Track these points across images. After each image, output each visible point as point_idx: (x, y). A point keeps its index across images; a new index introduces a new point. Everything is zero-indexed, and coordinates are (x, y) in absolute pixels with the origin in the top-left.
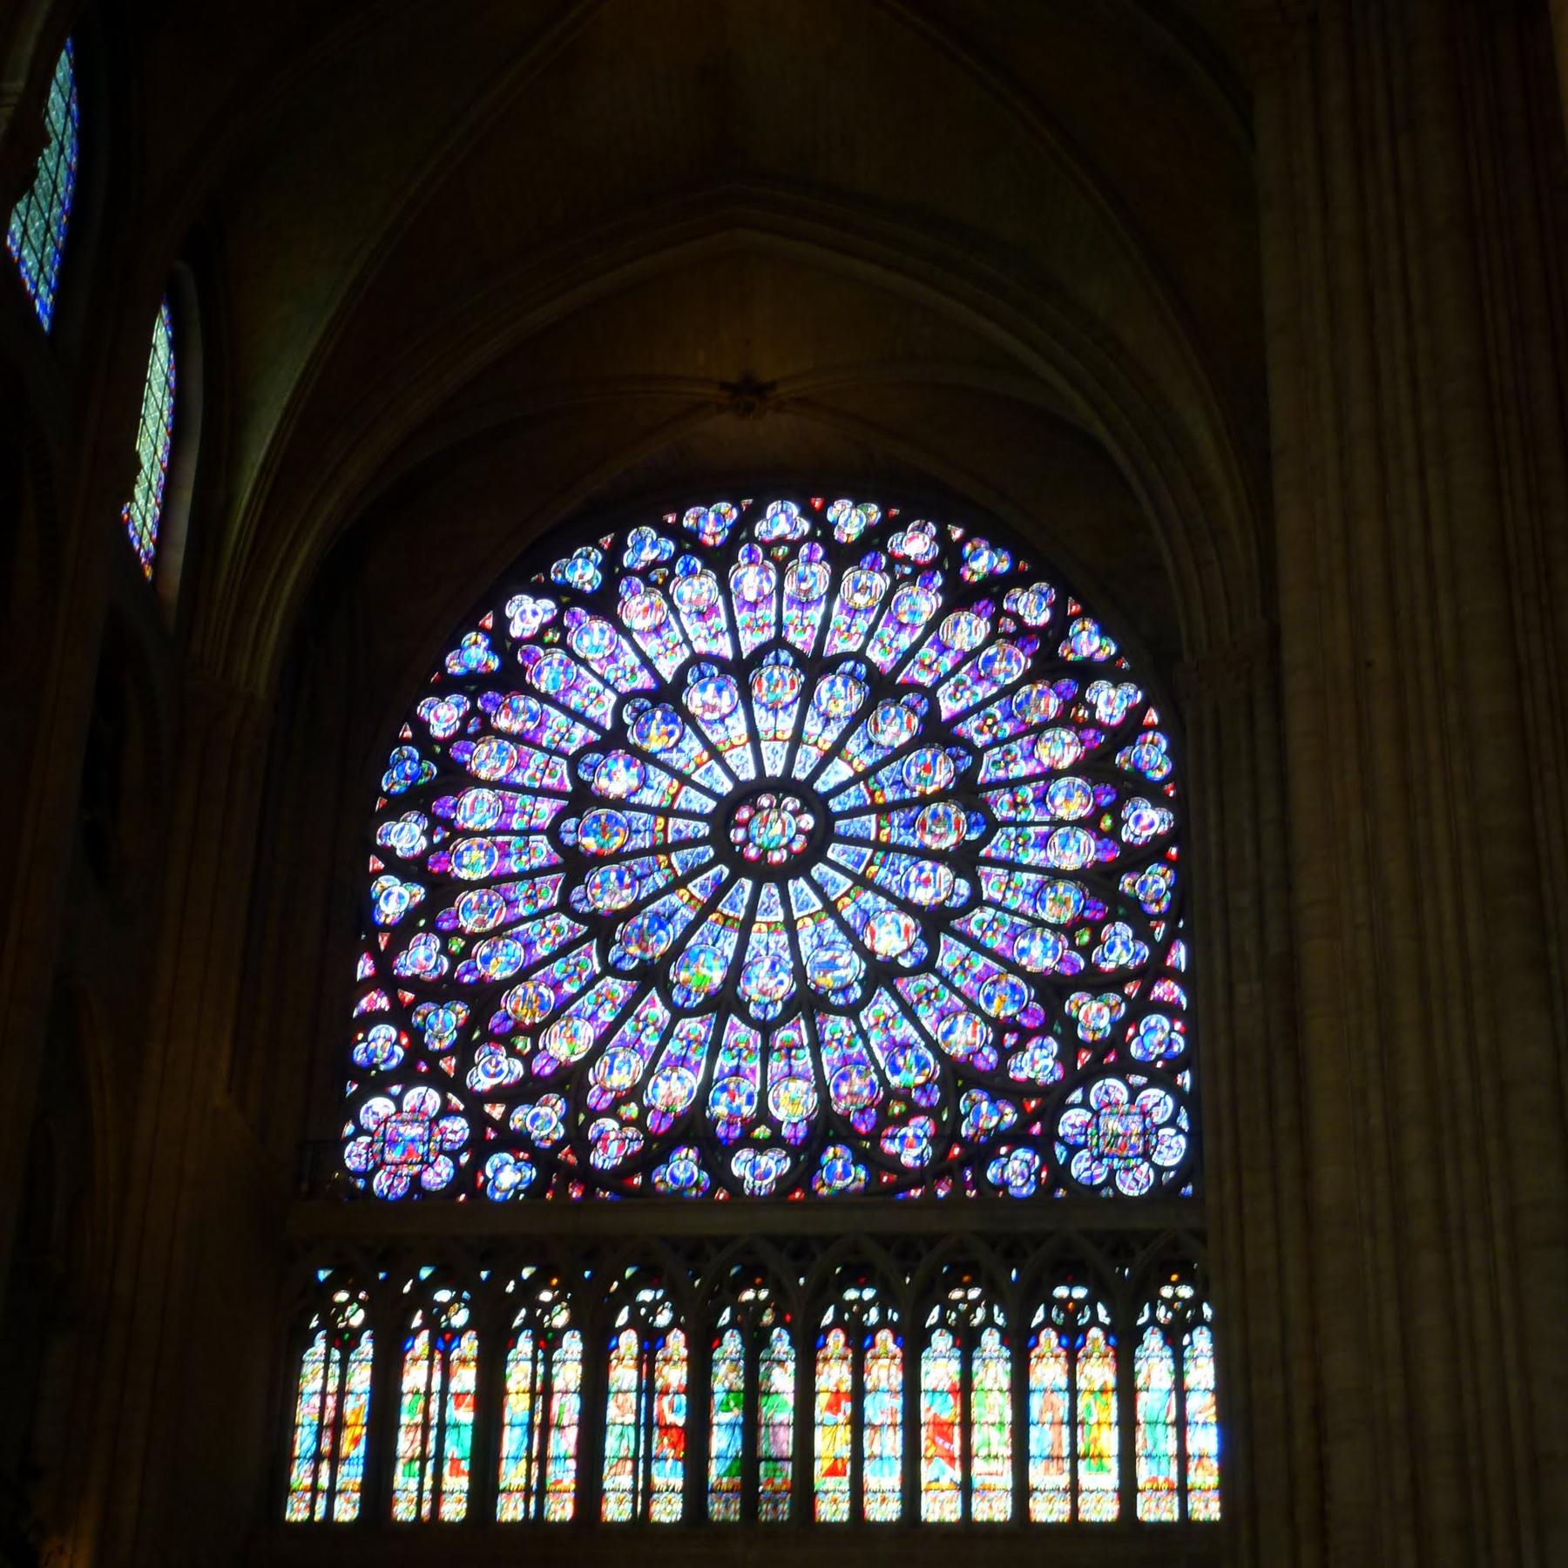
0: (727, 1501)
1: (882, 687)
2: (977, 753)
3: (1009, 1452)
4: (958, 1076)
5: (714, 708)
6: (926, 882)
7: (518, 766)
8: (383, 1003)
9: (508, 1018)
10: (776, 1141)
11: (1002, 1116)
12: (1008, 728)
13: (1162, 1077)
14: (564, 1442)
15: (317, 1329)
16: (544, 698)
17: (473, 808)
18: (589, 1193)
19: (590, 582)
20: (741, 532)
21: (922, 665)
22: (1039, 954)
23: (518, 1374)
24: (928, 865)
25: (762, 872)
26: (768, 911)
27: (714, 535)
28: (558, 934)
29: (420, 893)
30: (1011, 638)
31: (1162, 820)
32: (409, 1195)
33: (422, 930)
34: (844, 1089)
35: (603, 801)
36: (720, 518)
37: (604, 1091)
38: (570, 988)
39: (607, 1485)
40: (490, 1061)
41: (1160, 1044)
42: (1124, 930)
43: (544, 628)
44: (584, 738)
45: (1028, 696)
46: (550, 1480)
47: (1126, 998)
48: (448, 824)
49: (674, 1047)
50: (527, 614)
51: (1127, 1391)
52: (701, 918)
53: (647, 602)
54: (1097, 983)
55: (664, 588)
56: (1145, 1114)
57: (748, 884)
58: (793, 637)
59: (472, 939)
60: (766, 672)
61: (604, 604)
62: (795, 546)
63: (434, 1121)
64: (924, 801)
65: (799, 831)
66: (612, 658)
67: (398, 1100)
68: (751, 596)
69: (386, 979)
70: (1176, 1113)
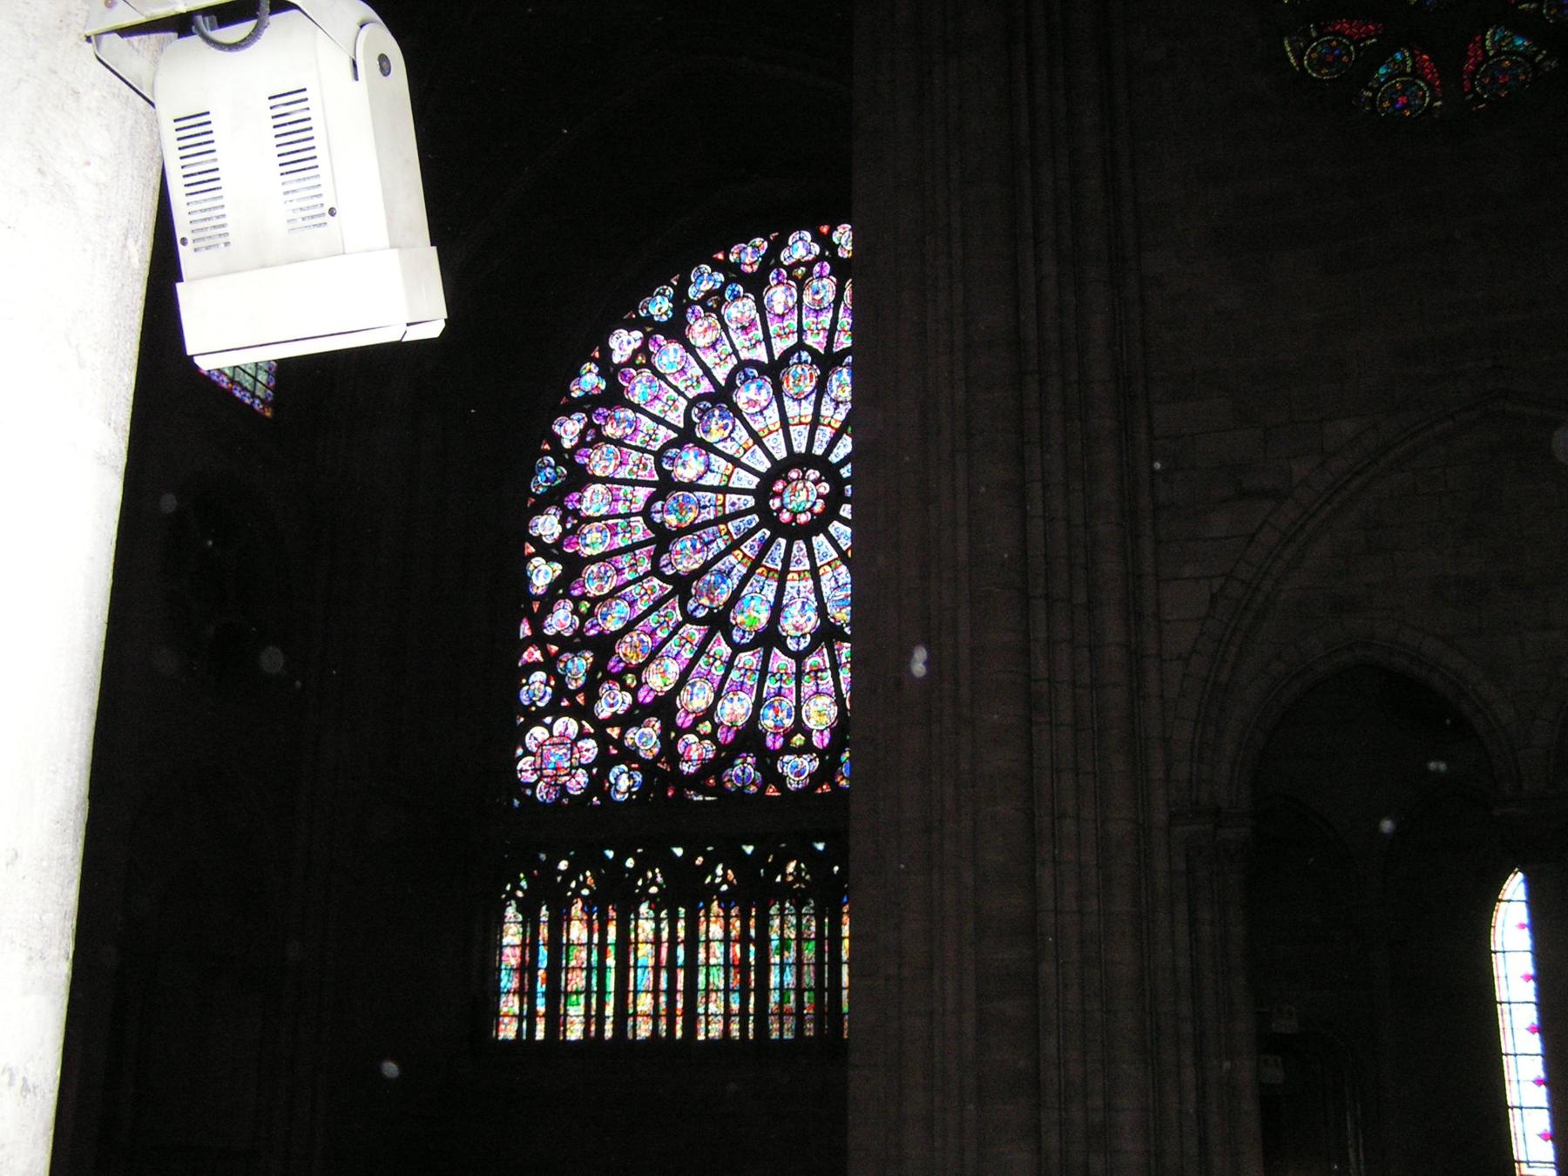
5: (755, 403)
7: (621, 463)
9: (621, 661)
10: (807, 748)
16: (636, 408)
20: (770, 260)
26: (798, 562)
27: (751, 264)
29: (558, 567)
36: (756, 248)
37: (688, 713)
43: (635, 353)
48: (576, 513)
49: (735, 675)
57: (783, 542)
58: (810, 340)
59: (595, 601)
60: (792, 370)
61: (676, 330)
63: (574, 742)
65: (819, 496)
66: (683, 371)
67: (550, 728)
68: (779, 309)
69: (539, 639)
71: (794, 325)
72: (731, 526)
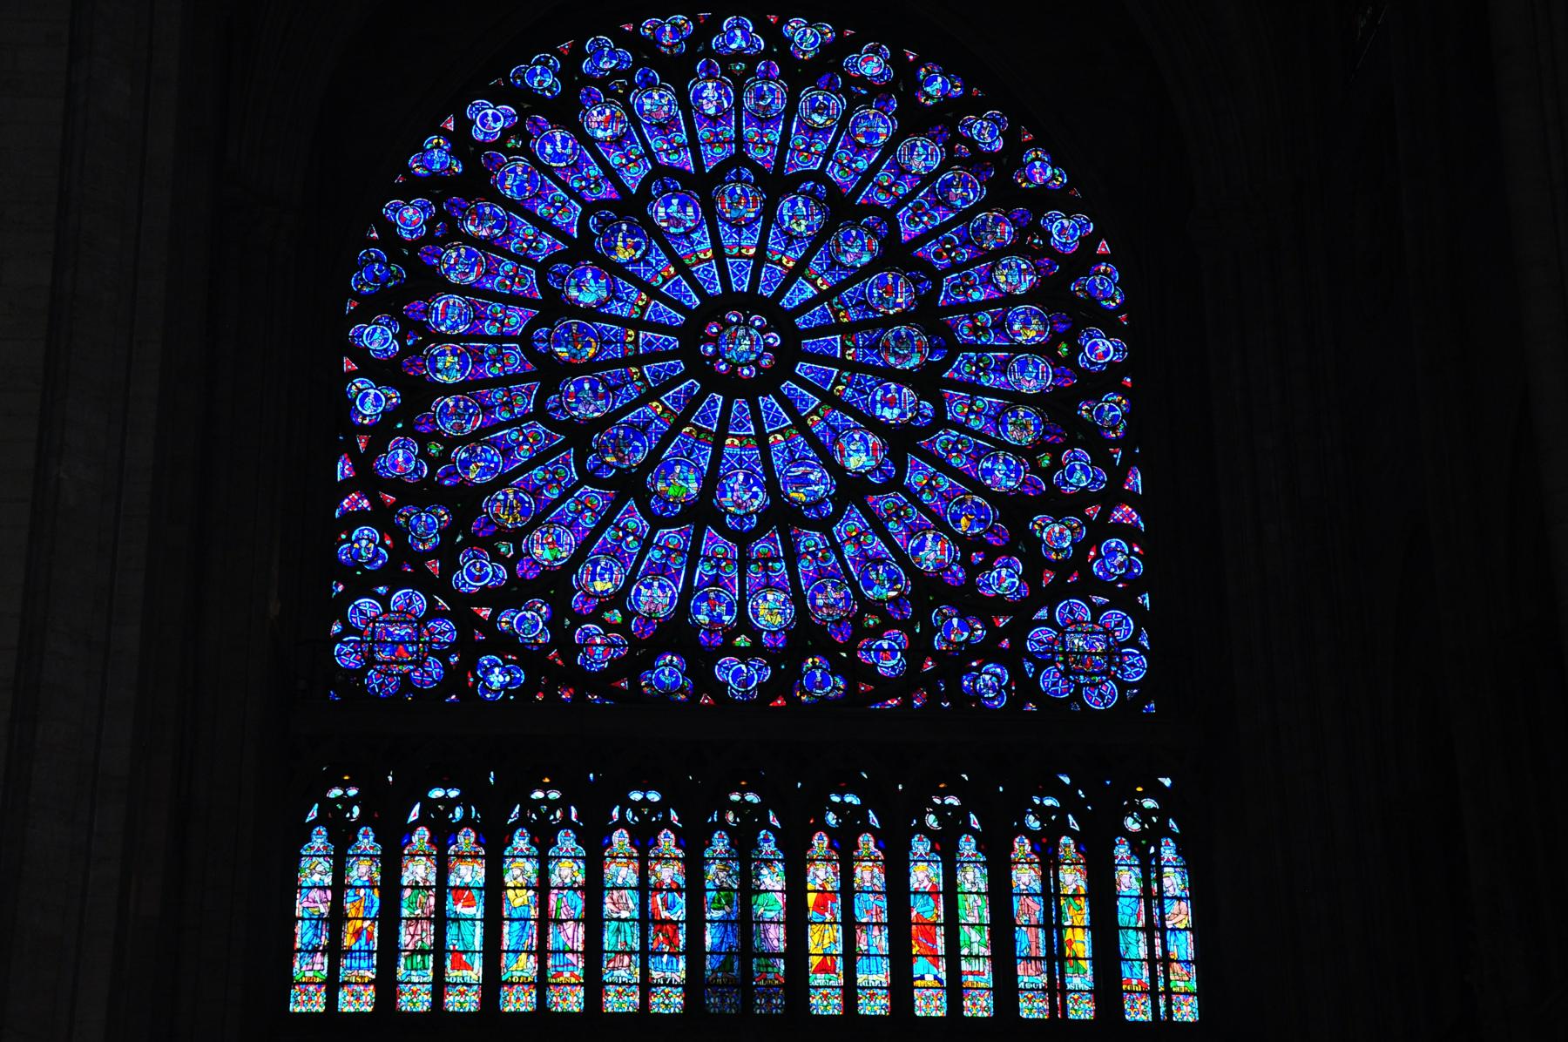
0: (722, 994)
1: (840, 209)
3: (988, 953)
4: (928, 590)
6: (890, 404)
7: (488, 273)
8: (365, 503)
9: (489, 522)
10: (756, 649)
12: (966, 254)
13: (1123, 599)
14: (571, 935)
15: (314, 824)
16: (509, 204)
17: (445, 314)
18: (579, 698)
19: (549, 89)
21: (882, 188)
22: (1003, 476)
23: (519, 871)
24: (893, 386)
25: (732, 386)
27: (671, 47)
28: (536, 442)
29: (395, 397)
30: (966, 164)
31: (1116, 350)
32: (398, 697)
34: (820, 602)
35: (574, 309)
36: (676, 29)
39: (605, 978)
40: (474, 565)
41: (1121, 565)
44: (554, 245)
45: (985, 221)
46: (551, 972)
47: (1087, 521)
49: (655, 554)
50: (490, 119)
51: (1102, 896)
52: (675, 430)
53: (608, 112)
54: (1061, 505)
56: (1108, 632)
57: (720, 399)
59: (451, 443)
61: (566, 112)
64: (888, 322)
65: (768, 347)
66: (576, 168)
67: (385, 600)
68: (712, 111)
69: (367, 480)
70: (1137, 633)
71: (730, 132)
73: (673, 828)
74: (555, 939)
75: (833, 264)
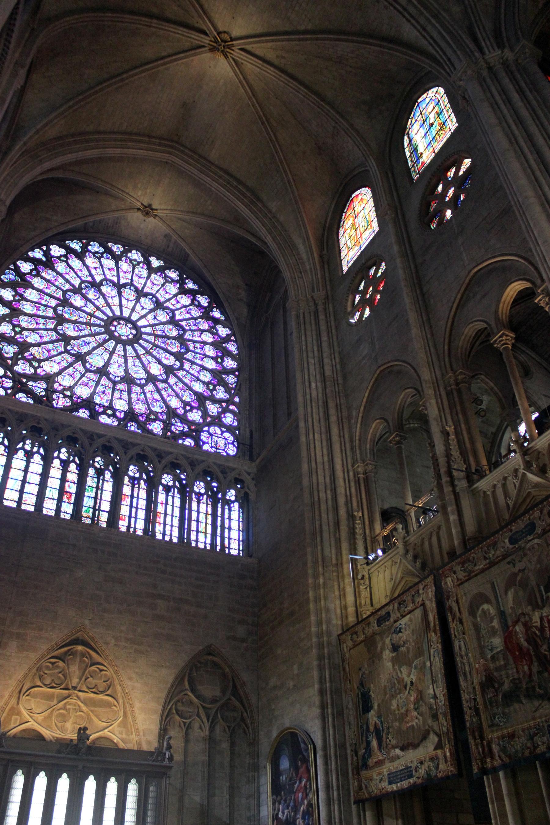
1: (159, 305)
2: (185, 331)
4: (171, 413)
6: (167, 359)
9: (32, 355)
11: (184, 428)
22: (198, 387)
24: (168, 355)
25: (118, 340)
29: (8, 311)
30: (197, 306)
33: (7, 321)
35: (72, 305)
36: (118, 248)
38: (53, 353)
42: (223, 389)
43: (61, 256)
46: (24, 499)
47: (222, 406)
48: (21, 295)
49: (84, 379)
50: (56, 251)
55: (99, 259)
57: (114, 343)
58: (135, 283)
59: (23, 329)
60: (126, 290)
62: (139, 263)
64: (169, 338)
65: (131, 333)
72: (93, 329)
73: (76, 463)
74: (27, 488)
75: (155, 318)
